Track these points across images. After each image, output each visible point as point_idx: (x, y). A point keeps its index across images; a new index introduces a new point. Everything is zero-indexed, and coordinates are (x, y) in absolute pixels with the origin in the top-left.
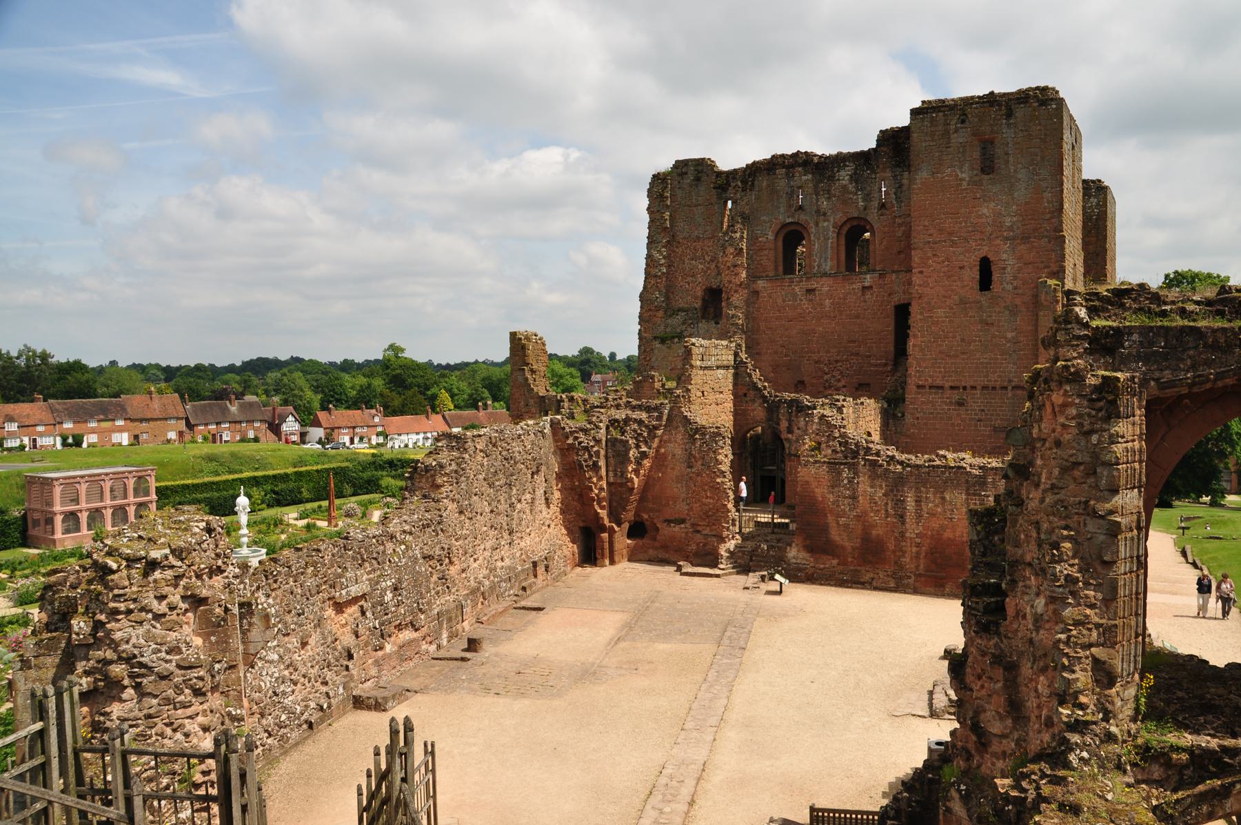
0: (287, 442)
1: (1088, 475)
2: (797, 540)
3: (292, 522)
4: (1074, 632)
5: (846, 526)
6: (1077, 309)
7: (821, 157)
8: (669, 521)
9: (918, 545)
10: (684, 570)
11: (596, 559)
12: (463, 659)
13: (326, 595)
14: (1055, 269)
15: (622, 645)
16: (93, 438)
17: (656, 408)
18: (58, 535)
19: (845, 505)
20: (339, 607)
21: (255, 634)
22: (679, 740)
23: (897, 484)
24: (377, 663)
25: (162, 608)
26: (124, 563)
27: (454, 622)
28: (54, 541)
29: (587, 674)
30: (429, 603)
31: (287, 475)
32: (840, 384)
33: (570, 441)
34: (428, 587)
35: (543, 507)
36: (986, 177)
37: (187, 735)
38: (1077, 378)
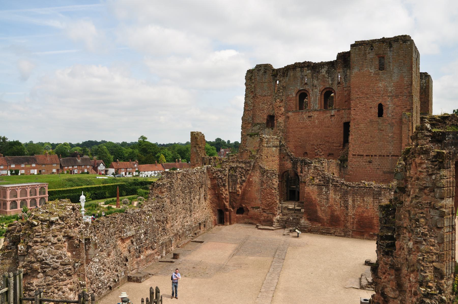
0: (100, 174)
1: (431, 192)
2: (305, 216)
3: (102, 206)
4: (426, 256)
5: (324, 210)
6: (426, 125)
7: (315, 63)
8: (253, 208)
9: (353, 219)
10: (259, 227)
11: (224, 222)
12: (172, 262)
13: (118, 236)
14: (409, 108)
15: (235, 257)
16: (23, 171)
17: (249, 163)
18: (8, 210)
19: (324, 202)
20: (123, 240)
21: (91, 251)
22: (259, 296)
23: (345, 194)
24: (137, 263)
25: (55, 240)
26: (40, 222)
27: (168, 247)
28: (6, 212)
29: (221, 269)
30: (158, 239)
31: (100, 187)
32: (321, 154)
33: (214, 175)
34: (158, 233)
35: (204, 201)
36: (381, 72)
37: (63, 292)
38: (426, 152)
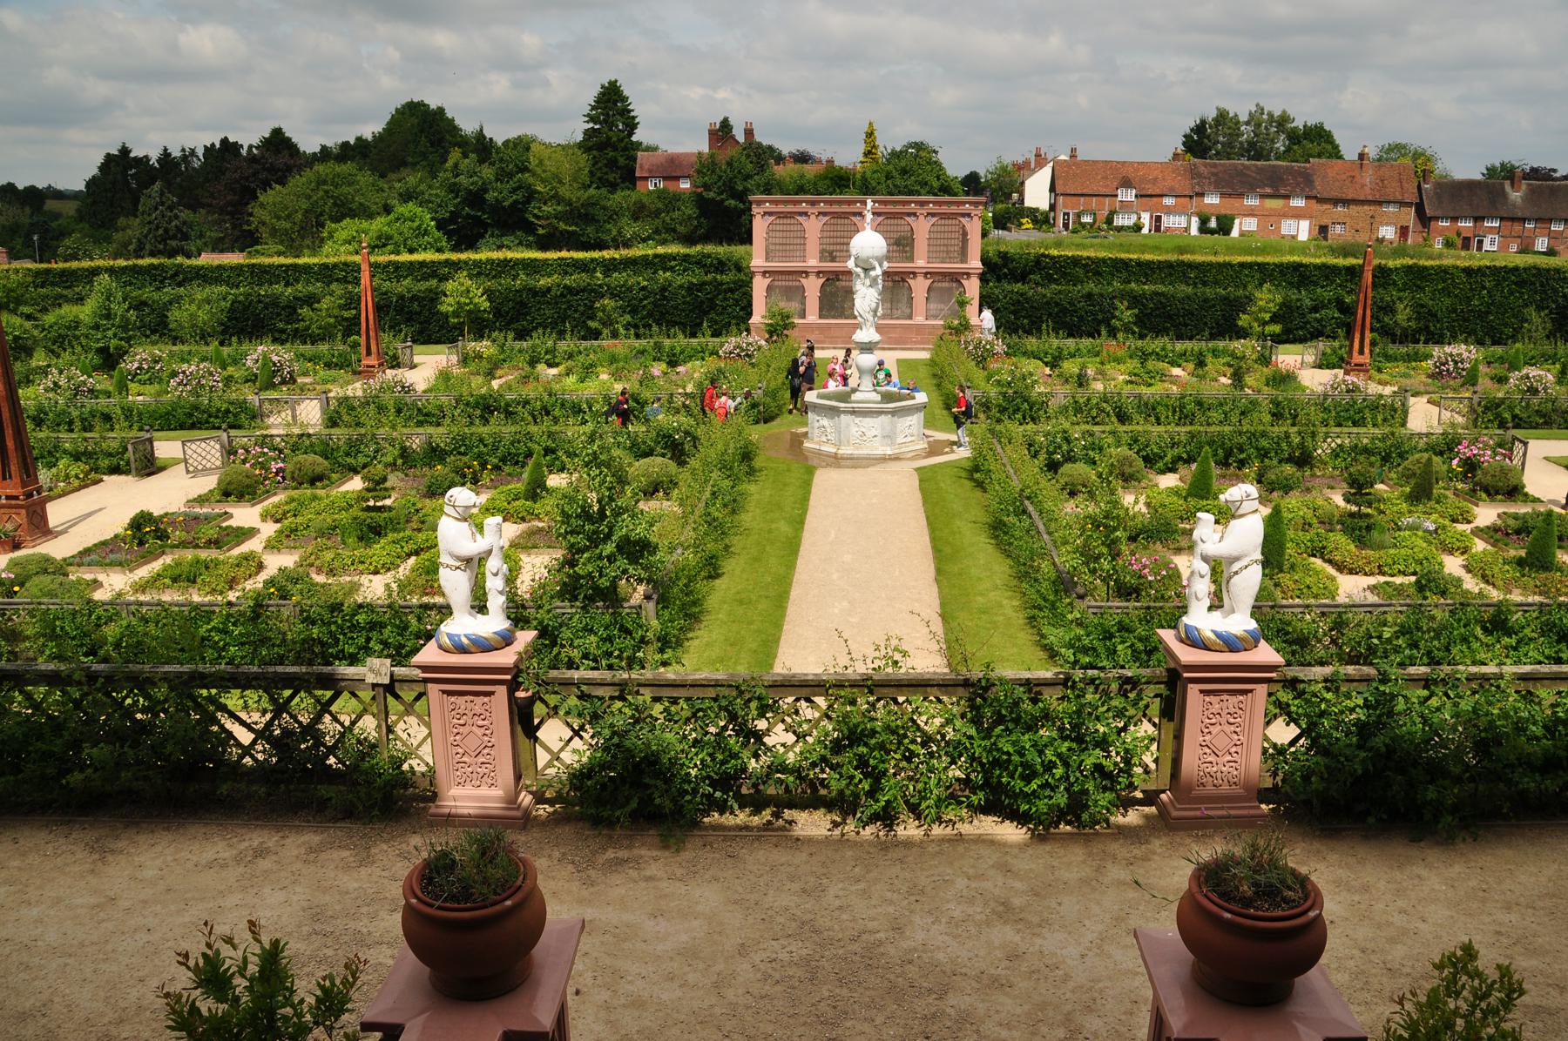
16: (1250, 224)
